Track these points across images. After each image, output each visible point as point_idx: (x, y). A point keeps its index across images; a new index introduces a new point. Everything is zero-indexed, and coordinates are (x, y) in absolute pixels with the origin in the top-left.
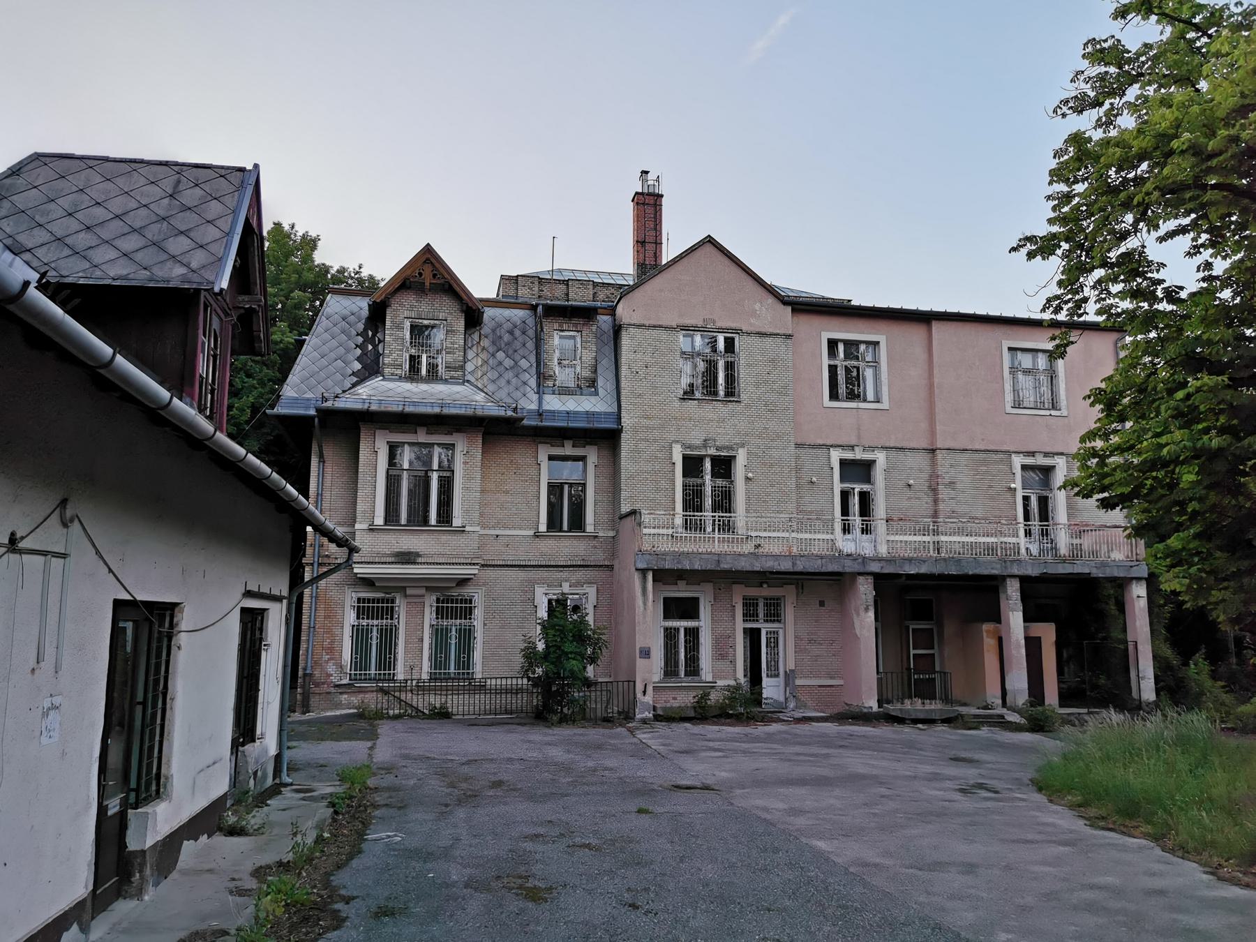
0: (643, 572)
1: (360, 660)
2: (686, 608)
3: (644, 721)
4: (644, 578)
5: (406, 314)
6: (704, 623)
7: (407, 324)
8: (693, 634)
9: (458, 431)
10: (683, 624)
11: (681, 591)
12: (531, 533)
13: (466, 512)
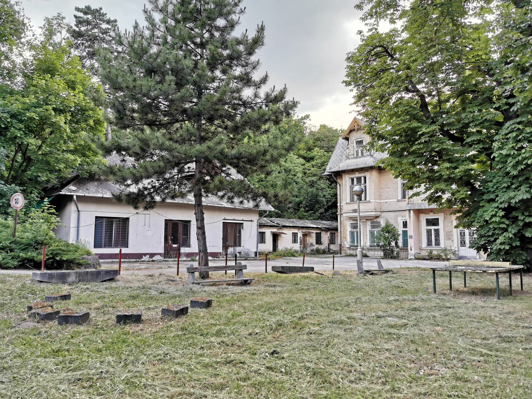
0: (409, 210)
1: (353, 241)
2: (434, 222)
3: (411, 259)
4: (410, 212)
5: (354, 138)
6: (441, 227)
7: (355, 141)
8: (437, 231)
9: (367, 171)
10: (433, 228)
11: (431, 216)
12: (396, 200)
13: (370, 196)
